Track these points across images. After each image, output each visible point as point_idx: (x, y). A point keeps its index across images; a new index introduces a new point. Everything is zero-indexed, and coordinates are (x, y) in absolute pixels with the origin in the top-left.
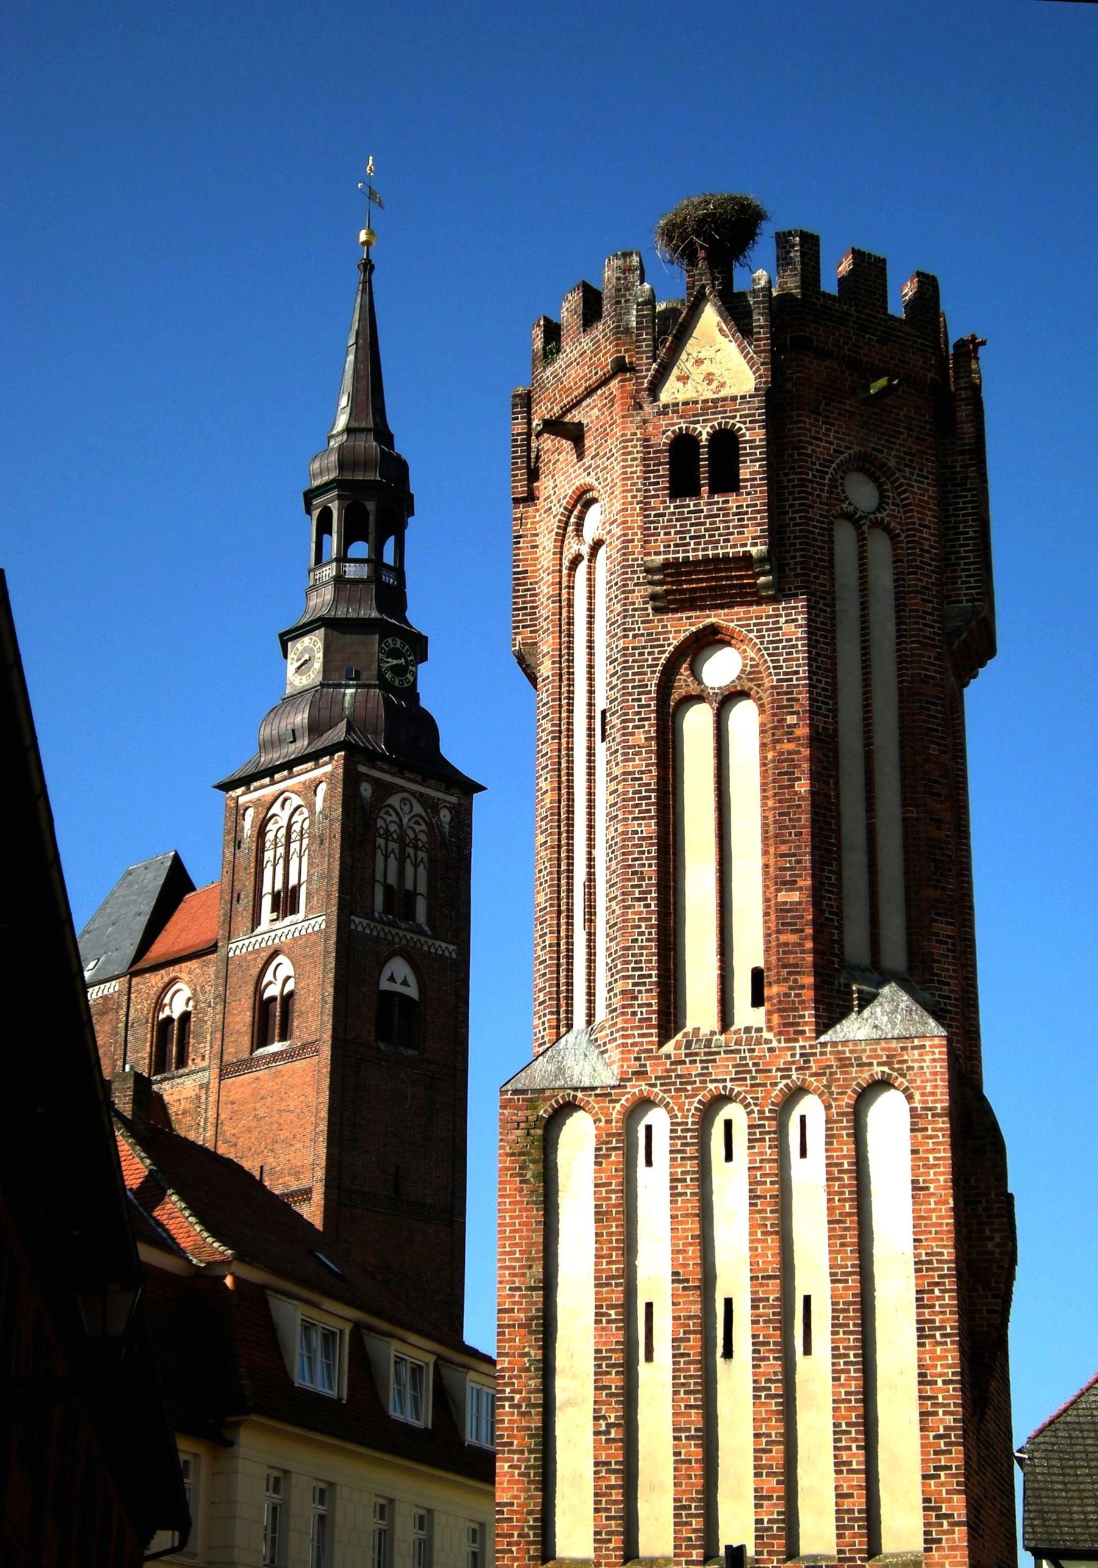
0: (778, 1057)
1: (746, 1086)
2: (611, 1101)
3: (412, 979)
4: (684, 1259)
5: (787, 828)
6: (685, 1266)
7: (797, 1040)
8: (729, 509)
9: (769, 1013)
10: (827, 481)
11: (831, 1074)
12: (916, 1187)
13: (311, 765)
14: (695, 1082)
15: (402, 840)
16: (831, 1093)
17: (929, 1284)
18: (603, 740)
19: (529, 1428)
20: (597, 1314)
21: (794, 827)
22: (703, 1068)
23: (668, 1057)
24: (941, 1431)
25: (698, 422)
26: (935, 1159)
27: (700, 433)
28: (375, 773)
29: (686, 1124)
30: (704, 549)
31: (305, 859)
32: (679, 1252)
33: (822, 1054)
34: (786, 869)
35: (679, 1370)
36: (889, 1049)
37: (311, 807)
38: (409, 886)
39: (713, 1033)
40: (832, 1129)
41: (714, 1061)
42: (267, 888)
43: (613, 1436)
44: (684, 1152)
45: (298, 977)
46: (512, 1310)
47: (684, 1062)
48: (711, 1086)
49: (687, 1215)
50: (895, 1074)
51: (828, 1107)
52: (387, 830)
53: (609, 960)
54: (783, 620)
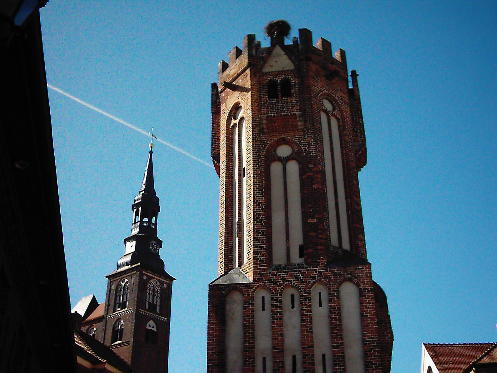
0: (311, 273)
1: (299, 282)
3: (155, 326)
8: (288, 101)
9: (305, 259)
10: (318, 98)
14: (280, 281)
15: (154, 291)
16: (330, 284)
22: (283, 277)
23: (270, 273)
25: (277, 77)
26: (369, 306)
27: (278, 80)
28: (147, 274)
29: (278, 295)
33: (326, 271)
38: (155, 303)
39: (286, 266)
48: (286, 283)
49: (278, 326)
51: (329, 289)
52: (150, 288)
53: (248, 243)
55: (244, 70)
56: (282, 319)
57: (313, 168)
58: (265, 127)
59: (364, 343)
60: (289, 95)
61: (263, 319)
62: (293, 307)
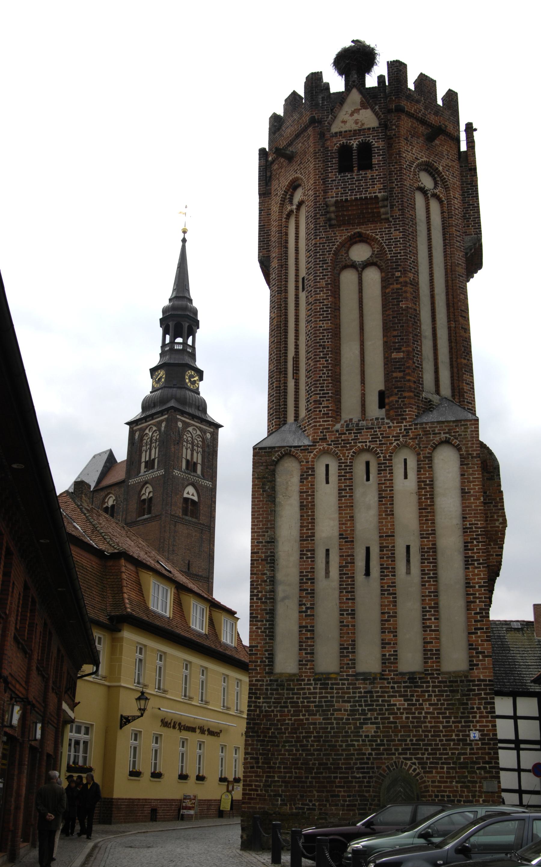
2: (309, 452)
3: (195, 494)
4: (346, 527)
5: (396, 323)
6: (346, 531)
7: (402, 423)
11: (420, 438)
12: (463, 491)
13: (160, 415)
15: (192, 443)
16: (420, 447)
17: (471, 539)
18: (303, 291)
19: (266, 610)
20: (301, 554)
21: (400, 323)
23: (337, 431)
24: (478, 611)
26: (473, 478)
30: (355, 195)
31: (157, 449)
32: (343, 524)
34: (396, 343)
35: (343, 581)
36: (449, 426)
37: (159, 430)
38: (195, 460)
39: (359, 421)
40: (420, 464)
41: (361, 433)
42: (143, 460)
43: (309, 613)
44: (346, 476)
45: (153, 492)
46: (258, 553)
47: (345, 434)
48: (359, 445)
49: (347, 506)
50: (452, 438)
51: (419, 454)
54: (393, 229)
55: (305, 129)
56: (352, 496)
57: (400, 277)
58: (333, 216)
59: (465, 530)
60: (369, 166)
61: (327, 496)
62: (368, 479)
